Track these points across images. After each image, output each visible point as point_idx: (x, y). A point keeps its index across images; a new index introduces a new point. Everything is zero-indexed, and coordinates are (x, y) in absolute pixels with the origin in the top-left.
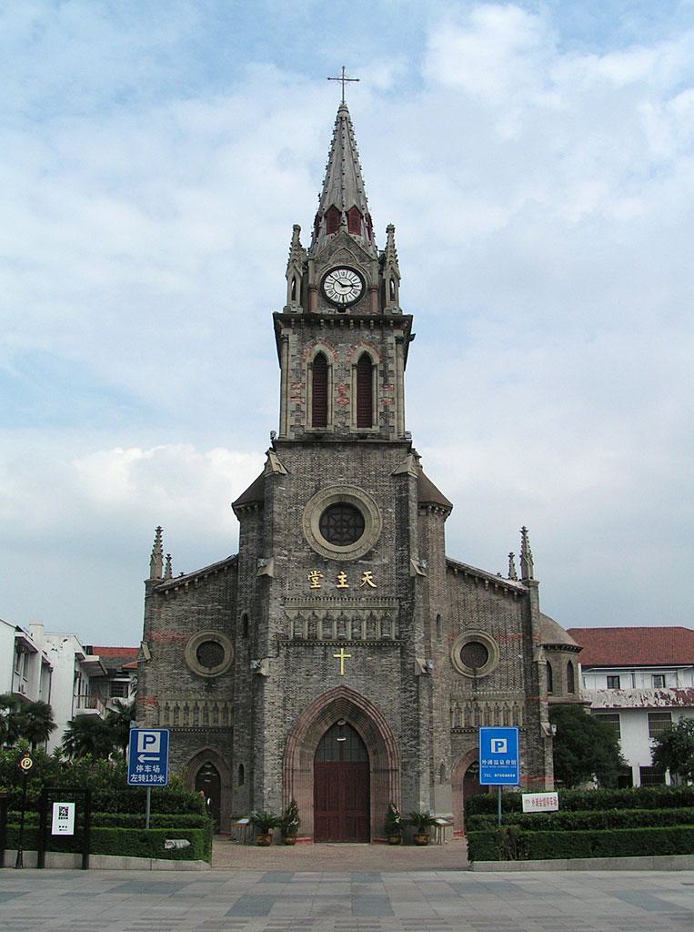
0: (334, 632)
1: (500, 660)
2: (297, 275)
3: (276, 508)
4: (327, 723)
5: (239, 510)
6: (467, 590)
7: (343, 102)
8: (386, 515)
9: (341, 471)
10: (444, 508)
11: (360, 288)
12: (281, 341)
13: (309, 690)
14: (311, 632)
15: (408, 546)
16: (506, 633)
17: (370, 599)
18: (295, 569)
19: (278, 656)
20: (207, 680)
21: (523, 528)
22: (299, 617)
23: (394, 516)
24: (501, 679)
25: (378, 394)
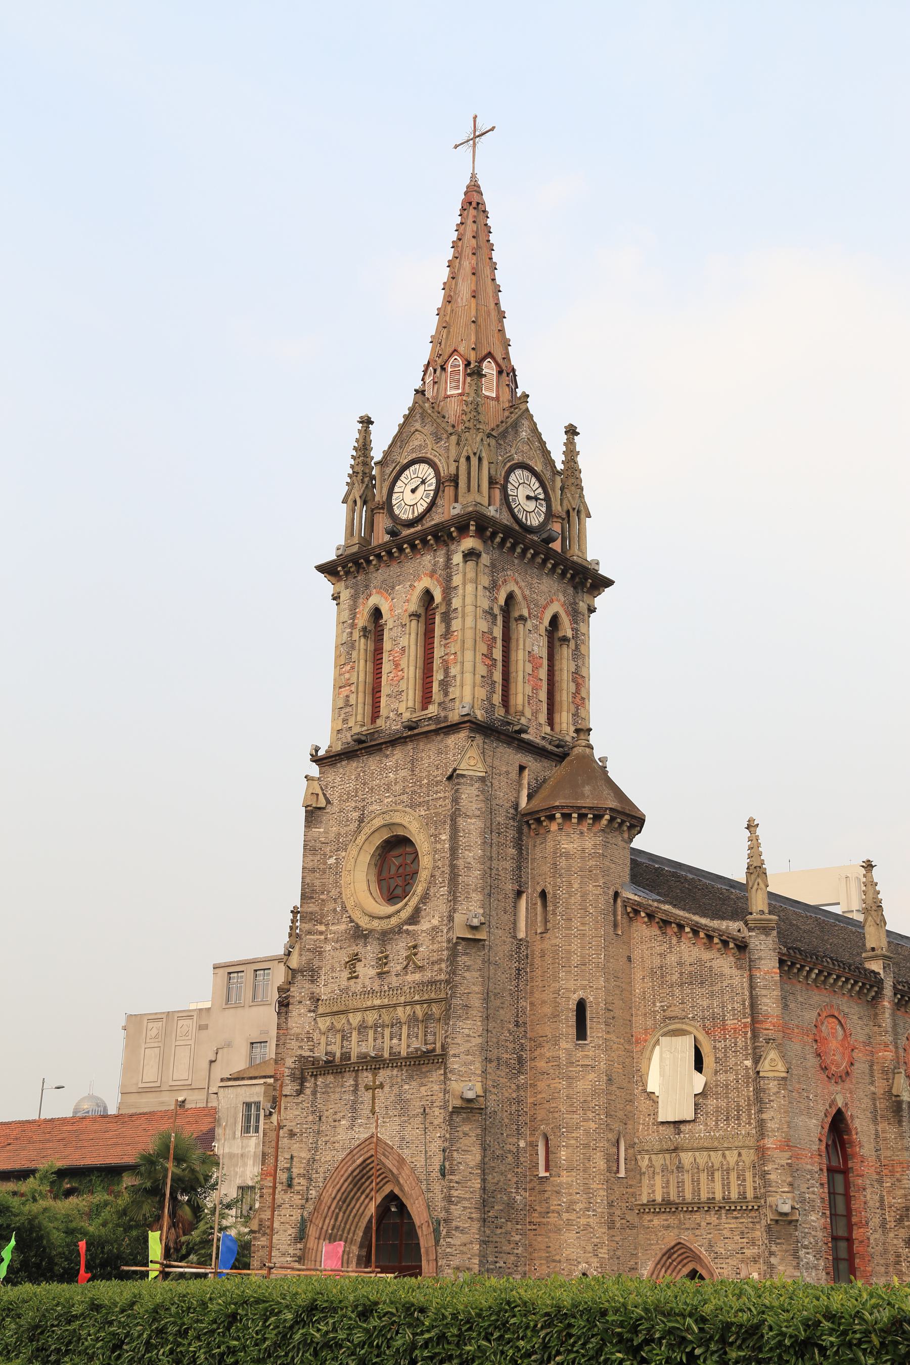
0: (368, 1047)
1: (716, 1072)
7: (473, 176)
8: (439, 846)
13: (336, 1145)
14: (344, 1050)
16: (724, 1020)
18: (332, 953)
19: (300, 1092)
21: (751, 820)
22: (331, 1028)
23: (447, 846)
24: (718, 1110)
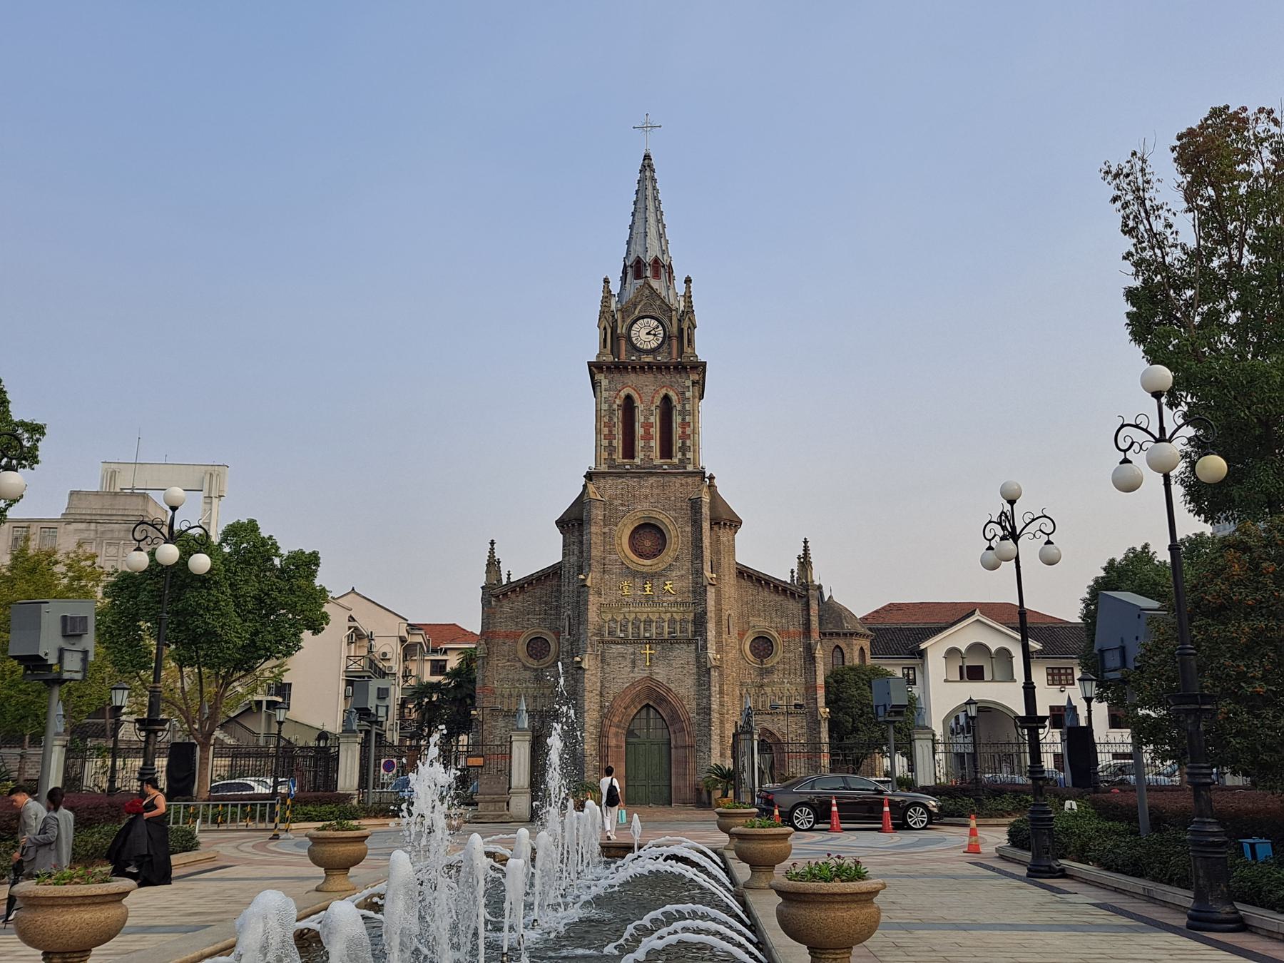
2: (607, 326)
3: (593, 529)
4: (636, 708)
5: (563, 527)
6: (755, 592)
9: (646, 497)
10: (734, 523)
11: (662, 335)
12: (595, 384)
15: (702, 561)
17: (670, 604)
20: (536, 670)
21: (805, 539)
24: (784, 669)
25: (677, 430)
